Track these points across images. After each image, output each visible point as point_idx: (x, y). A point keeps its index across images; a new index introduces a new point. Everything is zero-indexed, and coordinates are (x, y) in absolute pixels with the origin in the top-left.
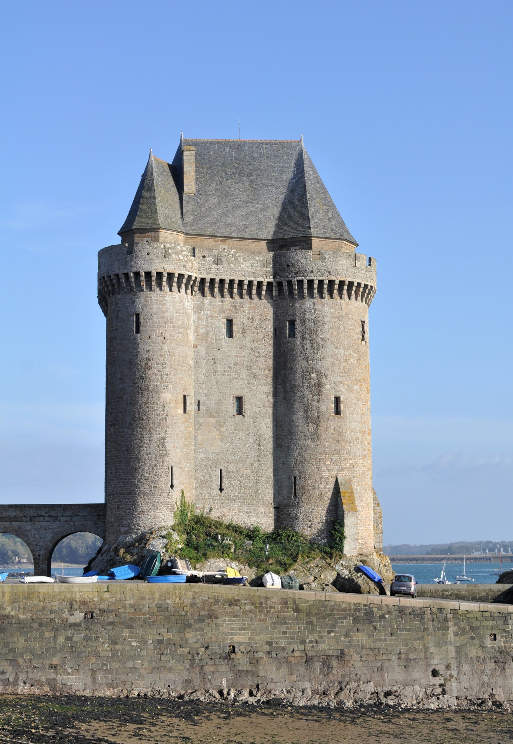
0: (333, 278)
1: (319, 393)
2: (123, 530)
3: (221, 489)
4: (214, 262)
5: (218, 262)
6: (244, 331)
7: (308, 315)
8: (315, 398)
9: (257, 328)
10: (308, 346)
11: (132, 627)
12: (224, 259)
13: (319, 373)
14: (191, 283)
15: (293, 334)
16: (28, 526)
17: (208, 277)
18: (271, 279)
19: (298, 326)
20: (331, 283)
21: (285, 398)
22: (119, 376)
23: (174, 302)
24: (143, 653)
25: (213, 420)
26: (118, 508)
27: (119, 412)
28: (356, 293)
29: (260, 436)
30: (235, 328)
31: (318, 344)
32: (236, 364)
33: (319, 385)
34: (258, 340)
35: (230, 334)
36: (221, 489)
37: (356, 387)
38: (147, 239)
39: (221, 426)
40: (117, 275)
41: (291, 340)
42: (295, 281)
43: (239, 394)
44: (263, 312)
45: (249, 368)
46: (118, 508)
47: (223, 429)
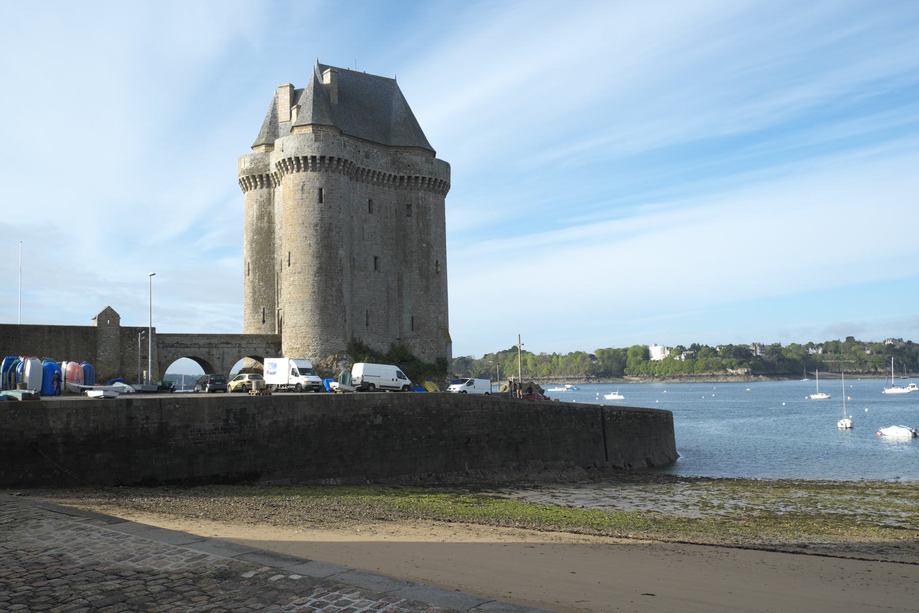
5: (367, 156)
13: (428, 244)
17: (362, 167)
19: (414, 209)
42: (413, 176)
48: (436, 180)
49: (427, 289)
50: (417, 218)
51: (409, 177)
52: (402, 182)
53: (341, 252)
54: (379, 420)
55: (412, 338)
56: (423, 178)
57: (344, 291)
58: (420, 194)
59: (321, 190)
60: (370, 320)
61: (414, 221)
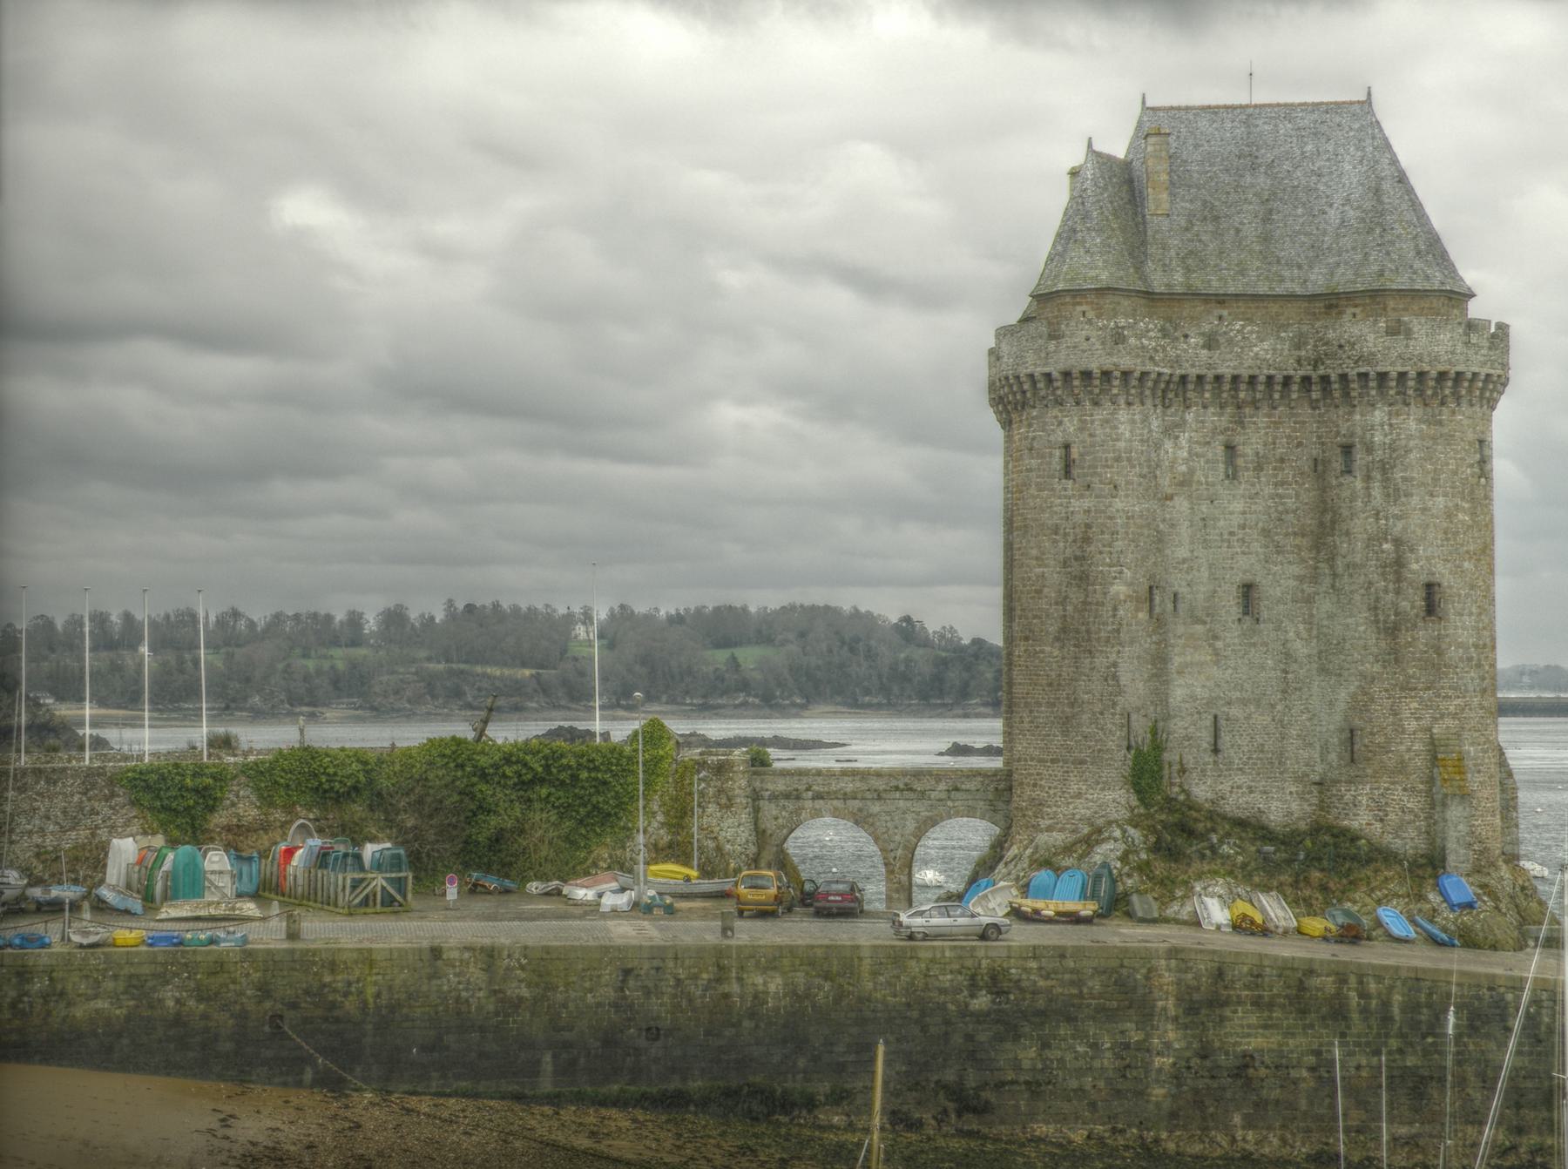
0: (1426, 368)
1: (1399, 579)
2: (1044, 823)
3: (1216, 751)
4: (1203, 347)
5: (1211, 343)
6: (1259, 468)
7: (1378, 438)
8: (1391, 586)
9: (1282, 460)
10: (1377, 491)
11: (1075, 1019)
12: (1222, 340)
14: (1163, 386)
15: (1349, 471)
16: (876, 808)
17: (1193, 372)
18: (1307, 370)
19: (1360, 458)
20: (1421, 375)
21: (1333, 586)
22: (1034, 552)
23: (1133, 422)
24: (1097, 1064)
25: (1199, 628)
26: (1035, 785)
27: (1035, 617)
28: (1470, 390)
29: (1288, 655)
30: (1240, 462)
31: (1397, 490)
32: (1243, 527)
33: (1399, 563)
34: (1283, 483)
35: (1232, 476)
36: (1216, 751)
37: (1466, 564)
38: (1084, 308)
39: (1216, 638)
40: (1031, 376)
41: (1346, 479)
42: (1352, 373)
43: (1248, 578)
44: (1295, 430)
45: (1266, 533)
46: (1035, 785)
47: (1219, 644)
48: (1421, 375)
49: (1394, 657)
50: (1368, 478)
51: (1344, 377)
52: (1325, 385)
53: (1119, 589)
54: (982, 1002)
55: (1350, 782)
56: (1383, 377)
57: (1124, 679)
58: (1379, 415)
59: (1067, 447)
60: (1226, 738)
61: (1359, 484)
